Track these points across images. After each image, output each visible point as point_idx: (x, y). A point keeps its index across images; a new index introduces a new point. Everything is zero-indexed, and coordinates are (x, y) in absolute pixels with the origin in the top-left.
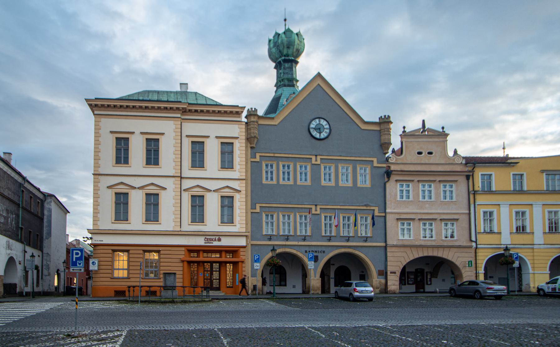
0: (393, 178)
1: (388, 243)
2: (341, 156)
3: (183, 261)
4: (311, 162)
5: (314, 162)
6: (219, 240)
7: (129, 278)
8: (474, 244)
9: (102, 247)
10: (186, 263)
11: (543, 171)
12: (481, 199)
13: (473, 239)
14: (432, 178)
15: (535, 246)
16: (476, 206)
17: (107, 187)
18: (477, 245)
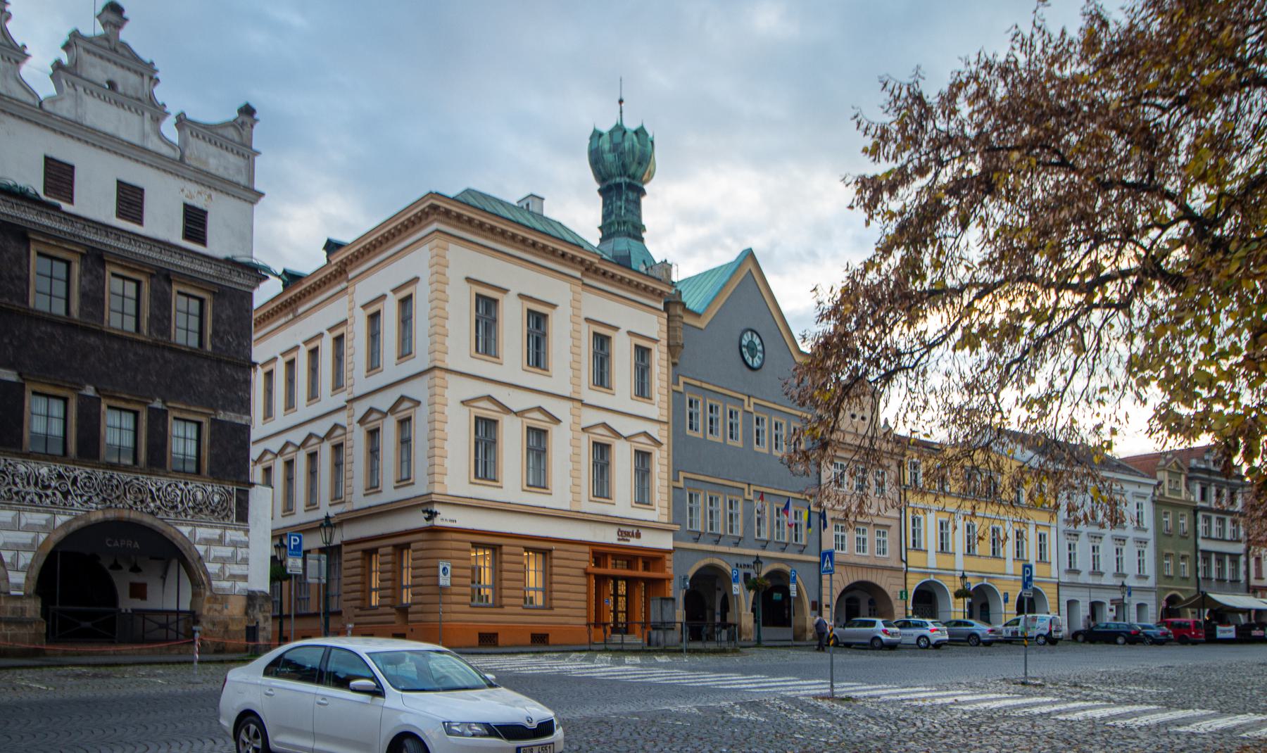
2: (775, 403)
3: (587, 574)
4: (743, 405)
6: (638, 536)
7: (502, 606)
8: (904, 565)
9: (455, 536)
10: (592, 578)
13: (904, 558)
17: (463, 402)
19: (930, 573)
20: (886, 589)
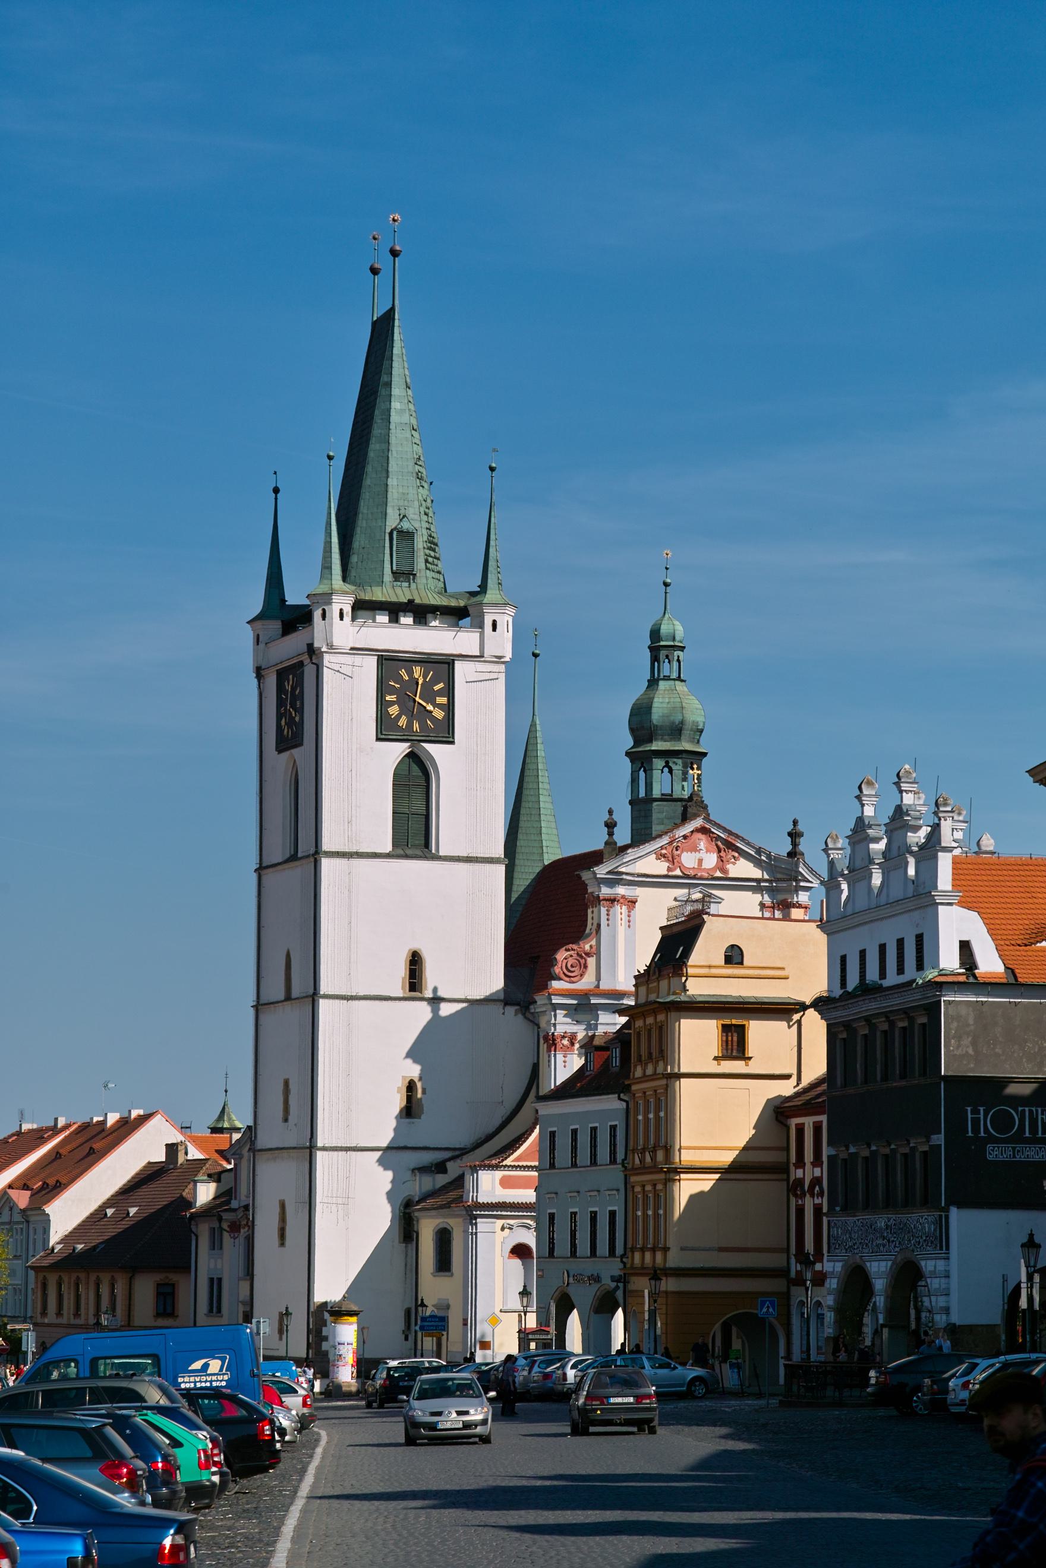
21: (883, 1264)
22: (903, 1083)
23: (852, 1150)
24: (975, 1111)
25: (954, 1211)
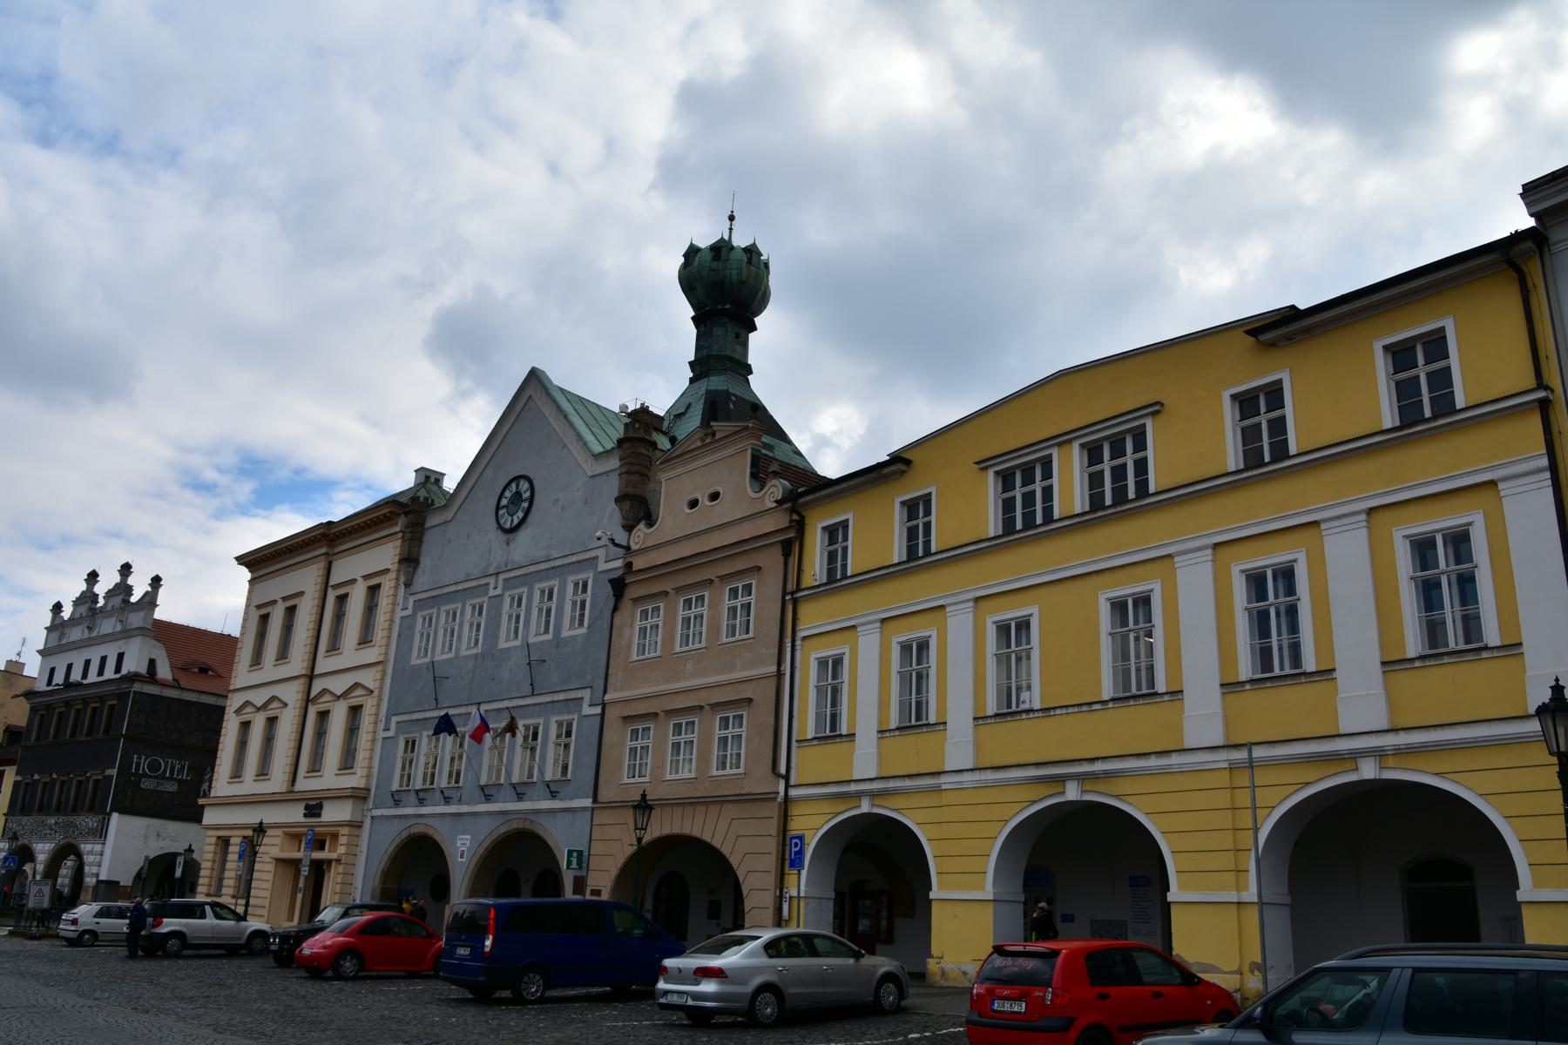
0: (632, 593)
1: (600, 798)
5: (492, 593)
8: (782, 784)
11: (983, 464)
12: (813, 618)
13: (783, 770)
14: (706, 574)
15: (944, 779)
16: (798, 643)
18: (787, 786)
19: (859, 795)
20: (726, 851)
21: (48, 845)
22: (89, 738)
23: (36, 777)
24: (139, 758)
25: (115, 816)
